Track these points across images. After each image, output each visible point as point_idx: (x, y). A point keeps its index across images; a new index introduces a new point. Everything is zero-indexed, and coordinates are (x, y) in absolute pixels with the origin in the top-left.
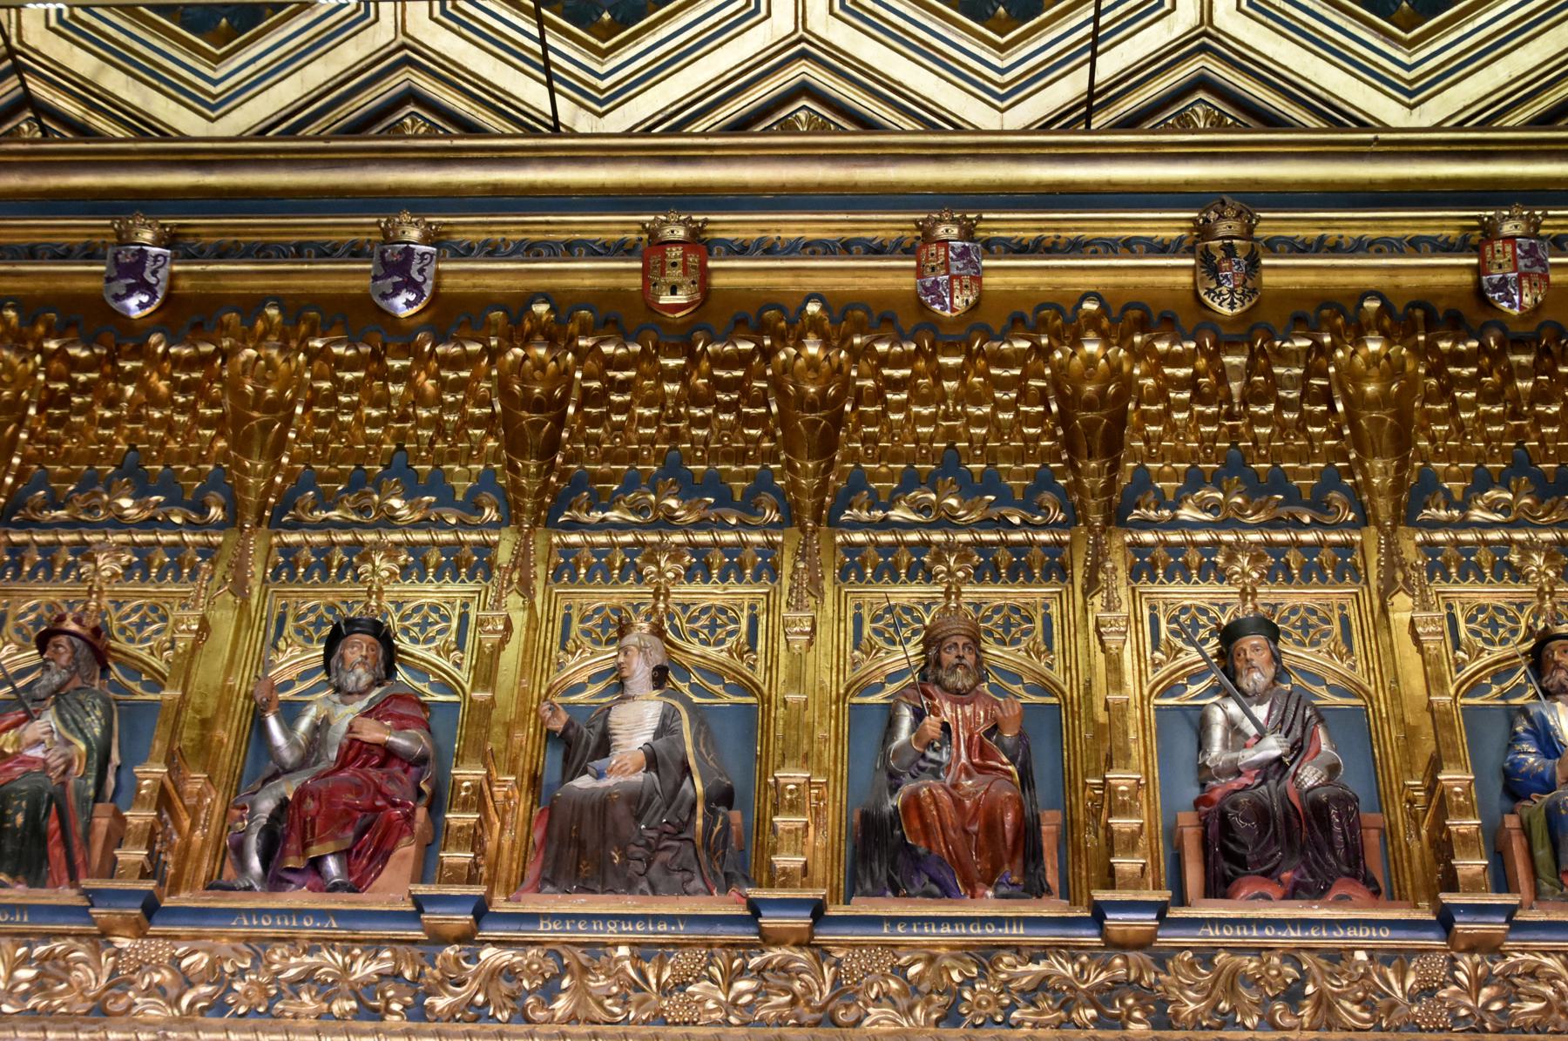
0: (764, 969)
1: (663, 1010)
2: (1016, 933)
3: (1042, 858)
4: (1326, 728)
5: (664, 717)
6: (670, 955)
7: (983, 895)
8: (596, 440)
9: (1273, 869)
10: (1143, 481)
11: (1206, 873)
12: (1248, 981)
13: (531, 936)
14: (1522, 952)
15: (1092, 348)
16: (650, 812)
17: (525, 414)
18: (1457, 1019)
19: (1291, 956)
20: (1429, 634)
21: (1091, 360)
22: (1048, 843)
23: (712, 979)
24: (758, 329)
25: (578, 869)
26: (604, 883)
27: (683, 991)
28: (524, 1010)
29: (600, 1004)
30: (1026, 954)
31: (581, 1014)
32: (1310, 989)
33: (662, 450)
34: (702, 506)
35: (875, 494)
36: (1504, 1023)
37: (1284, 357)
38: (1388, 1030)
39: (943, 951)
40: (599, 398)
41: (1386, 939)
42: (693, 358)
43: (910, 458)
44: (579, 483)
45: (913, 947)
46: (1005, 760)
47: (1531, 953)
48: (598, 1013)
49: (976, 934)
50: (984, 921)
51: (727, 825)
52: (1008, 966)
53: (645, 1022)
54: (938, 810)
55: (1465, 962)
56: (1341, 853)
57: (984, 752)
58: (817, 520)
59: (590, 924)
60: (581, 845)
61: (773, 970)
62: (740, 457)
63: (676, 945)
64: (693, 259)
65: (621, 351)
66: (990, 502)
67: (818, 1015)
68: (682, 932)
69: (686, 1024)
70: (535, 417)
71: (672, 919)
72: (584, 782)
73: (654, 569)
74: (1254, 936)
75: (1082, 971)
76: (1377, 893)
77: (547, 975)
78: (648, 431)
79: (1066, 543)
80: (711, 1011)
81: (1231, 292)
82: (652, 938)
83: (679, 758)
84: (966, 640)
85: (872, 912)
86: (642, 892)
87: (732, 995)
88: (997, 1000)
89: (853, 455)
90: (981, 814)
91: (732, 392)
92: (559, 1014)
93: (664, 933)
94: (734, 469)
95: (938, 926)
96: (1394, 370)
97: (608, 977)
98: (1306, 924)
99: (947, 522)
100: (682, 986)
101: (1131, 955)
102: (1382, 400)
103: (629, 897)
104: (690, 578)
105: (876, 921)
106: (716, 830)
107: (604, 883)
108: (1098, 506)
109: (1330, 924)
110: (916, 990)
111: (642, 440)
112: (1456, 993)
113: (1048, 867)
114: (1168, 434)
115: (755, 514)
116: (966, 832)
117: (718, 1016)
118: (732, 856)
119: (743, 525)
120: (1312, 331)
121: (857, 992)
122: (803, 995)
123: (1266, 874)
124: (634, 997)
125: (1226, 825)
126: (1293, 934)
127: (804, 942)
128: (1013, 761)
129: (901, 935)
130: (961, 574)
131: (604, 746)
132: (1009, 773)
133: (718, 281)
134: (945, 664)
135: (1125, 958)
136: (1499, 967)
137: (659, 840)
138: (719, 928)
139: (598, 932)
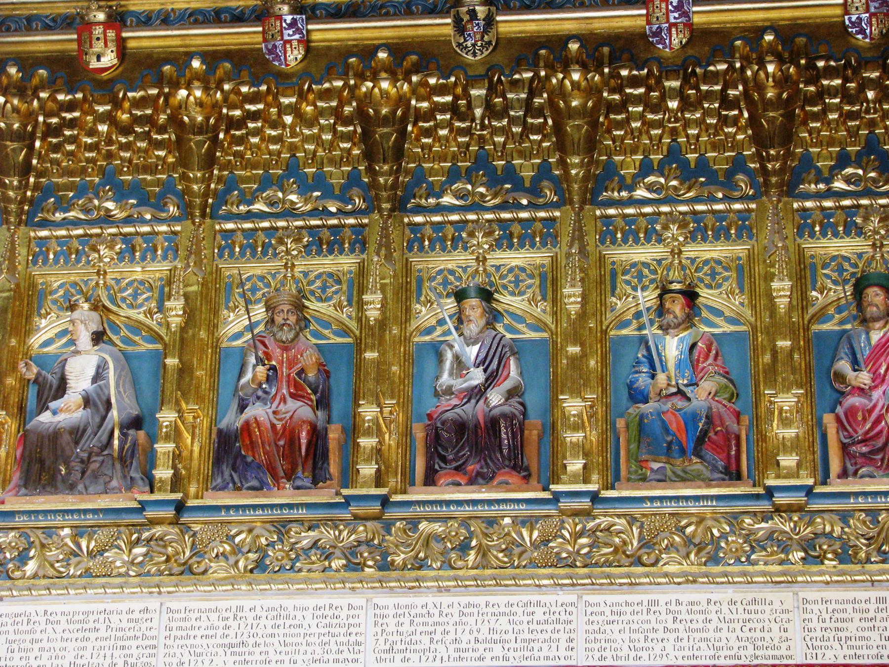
0: (151, 539)
1: (90, 568)
2: (302, 513)
3: (328, 456)
4: (518, 360)
5: (98, 367)
6: (95, 533)
7: (284, 488)
8: (57, 163)
9: (464, 463)
10: (419, 177)
11: (427, 464)
12: (439, 539)
13: (12, 525)
14: (605, 516)
15: (385, 85)
16: (83, 441)
17: (8, 143)
18: (561, 559)
19: (465, 522)
20: (572, 303)
21: (384, 94)
22: (333, 446)
23: (120, 549)
24: (159, 82)
25: (40, 479)
26: (56, 489)
27: (102, 555)
28: (7, 572)
29: (52, 566)
30: (306, 525)
31: (40, 574)
32: (474, 543)
33: (101, 166)
34: (128, 206)
35: (242, 192)
36: (588, 561)
37: (515, 85)
38: (518, 567)
39: (259, 524)
40: (55, 131)
41: (524, 510)
42: (117, 104)
43: (266, 166)
44: (47, 191)
45: (241, 523)
46: (309, 391)
47: (611, 516)
48: (51, 572)
49: (277, 514)
50: (281, 506)
51: (135, 444)
52: (296, 533)
53: (80, 576)
54: (259, 431)
55: (569, 523)
56: (505, 452)
57: (297, 386)
58: (203, 215)
59: (46, 516)
60: (42, 462)
61: (156, 540)
62: (151, 169)
63: (99, 527)
64: (111, 34)
65: (69, 97)
66: (317, 197)
67: (182, 568)
68: (101, 519)
69: (104, 576)
70: (15, 145)
71: (95, 511)
72: (45, 417)
73: (97, 255)
74: (444, 511)
75: (340, 535)
76: (527, 478)
77: (21, 549)
78: (91, 155)
79: (366, 225)
80: (119, 568)
81: (474, 45)
82: (83, 523)
83: (105, 398)
84: (290, 307)
85: (214, 503)
86: (80, 493)
87: (131, 557)
88: (288, 555)
89: (227, 166)
90: (287, 432)
91: (145, 125)
92: (28, 574)
93: (90, 519)
94: (149, 178)
95: (254, 511)
96: (592, 91)
97: (57, 549)
98: (475, 502)
99: (290, 213)
100: (101, 552)
101: (369, 524)
102: (582, 112)
103: (70, 497)
104: (121, 258)
105: (217, 508)
106: (126, 447)
107: (56, 489)
108: (389, 196)
109: (490, 502)
110: (240, 551)
111: (88, 160)
112: (561, 543)
113: (332, 462)
114: (436, 145)
115: (164, 211)
116: (277, 445)
117: (123, 570)
118: (135, 462)
119: (157, 220)
120: (534, 66)
121: (205, 553)
122: (174, 556)
123: (457, 469)
124: (74, 560)
125: (437, 436)
126: (467, 508)
127: (175, 522)
128: (315, 392)
129: (233, 516)
130: (295, 253)
131: (61, 388)
132: (311, 400)
133: (131, 44)
134: (277, 323)
135: (365, 526)
136: (591, 525)
137: (89, 458)
138: (124, 516)
139: (51, 520)
